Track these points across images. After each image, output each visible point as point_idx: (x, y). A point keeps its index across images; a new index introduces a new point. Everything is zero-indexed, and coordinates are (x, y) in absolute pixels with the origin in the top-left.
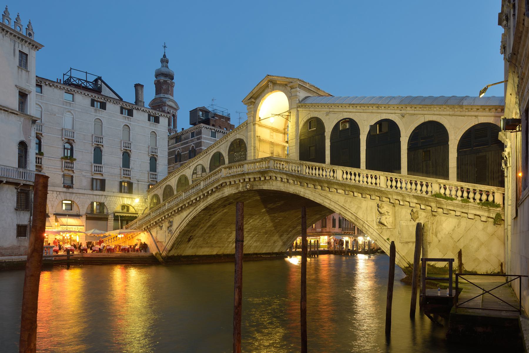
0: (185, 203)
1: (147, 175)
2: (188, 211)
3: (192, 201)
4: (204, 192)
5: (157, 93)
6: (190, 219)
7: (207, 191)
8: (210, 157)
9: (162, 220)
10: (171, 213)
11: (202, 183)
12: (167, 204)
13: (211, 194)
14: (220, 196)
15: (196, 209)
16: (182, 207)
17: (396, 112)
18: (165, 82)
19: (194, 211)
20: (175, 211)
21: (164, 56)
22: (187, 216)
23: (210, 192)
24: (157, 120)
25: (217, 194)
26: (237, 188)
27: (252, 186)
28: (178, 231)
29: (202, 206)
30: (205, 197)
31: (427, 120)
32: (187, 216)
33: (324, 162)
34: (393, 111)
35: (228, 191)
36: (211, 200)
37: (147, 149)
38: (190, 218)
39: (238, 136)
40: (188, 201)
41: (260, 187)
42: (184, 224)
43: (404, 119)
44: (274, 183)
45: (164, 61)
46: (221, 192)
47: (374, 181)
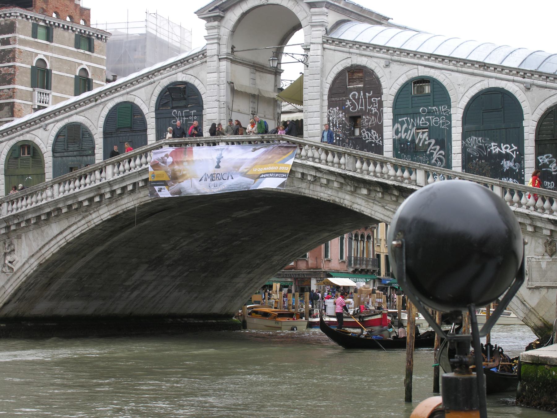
0: (60, 206)
2: (65, 224)
3: (81, 202)
4: (115, 188)
6: (70, 238)
10: (19, 224)
13: (133, 191)
15: (87, 219)
16: (49, 214)
17: (516, 78)
19: (83, 222)
20: (28, 221)
22: (61, 233)
23: (130, 188)
28: (34, 264)
29: (104, 213)
30: (114, 197)
32: (61, 233)
34: (511, 78)
36: (128, 203)
39: (181, 77)
40: (69, 202)
42: (54, 248)
43: (529, 93)
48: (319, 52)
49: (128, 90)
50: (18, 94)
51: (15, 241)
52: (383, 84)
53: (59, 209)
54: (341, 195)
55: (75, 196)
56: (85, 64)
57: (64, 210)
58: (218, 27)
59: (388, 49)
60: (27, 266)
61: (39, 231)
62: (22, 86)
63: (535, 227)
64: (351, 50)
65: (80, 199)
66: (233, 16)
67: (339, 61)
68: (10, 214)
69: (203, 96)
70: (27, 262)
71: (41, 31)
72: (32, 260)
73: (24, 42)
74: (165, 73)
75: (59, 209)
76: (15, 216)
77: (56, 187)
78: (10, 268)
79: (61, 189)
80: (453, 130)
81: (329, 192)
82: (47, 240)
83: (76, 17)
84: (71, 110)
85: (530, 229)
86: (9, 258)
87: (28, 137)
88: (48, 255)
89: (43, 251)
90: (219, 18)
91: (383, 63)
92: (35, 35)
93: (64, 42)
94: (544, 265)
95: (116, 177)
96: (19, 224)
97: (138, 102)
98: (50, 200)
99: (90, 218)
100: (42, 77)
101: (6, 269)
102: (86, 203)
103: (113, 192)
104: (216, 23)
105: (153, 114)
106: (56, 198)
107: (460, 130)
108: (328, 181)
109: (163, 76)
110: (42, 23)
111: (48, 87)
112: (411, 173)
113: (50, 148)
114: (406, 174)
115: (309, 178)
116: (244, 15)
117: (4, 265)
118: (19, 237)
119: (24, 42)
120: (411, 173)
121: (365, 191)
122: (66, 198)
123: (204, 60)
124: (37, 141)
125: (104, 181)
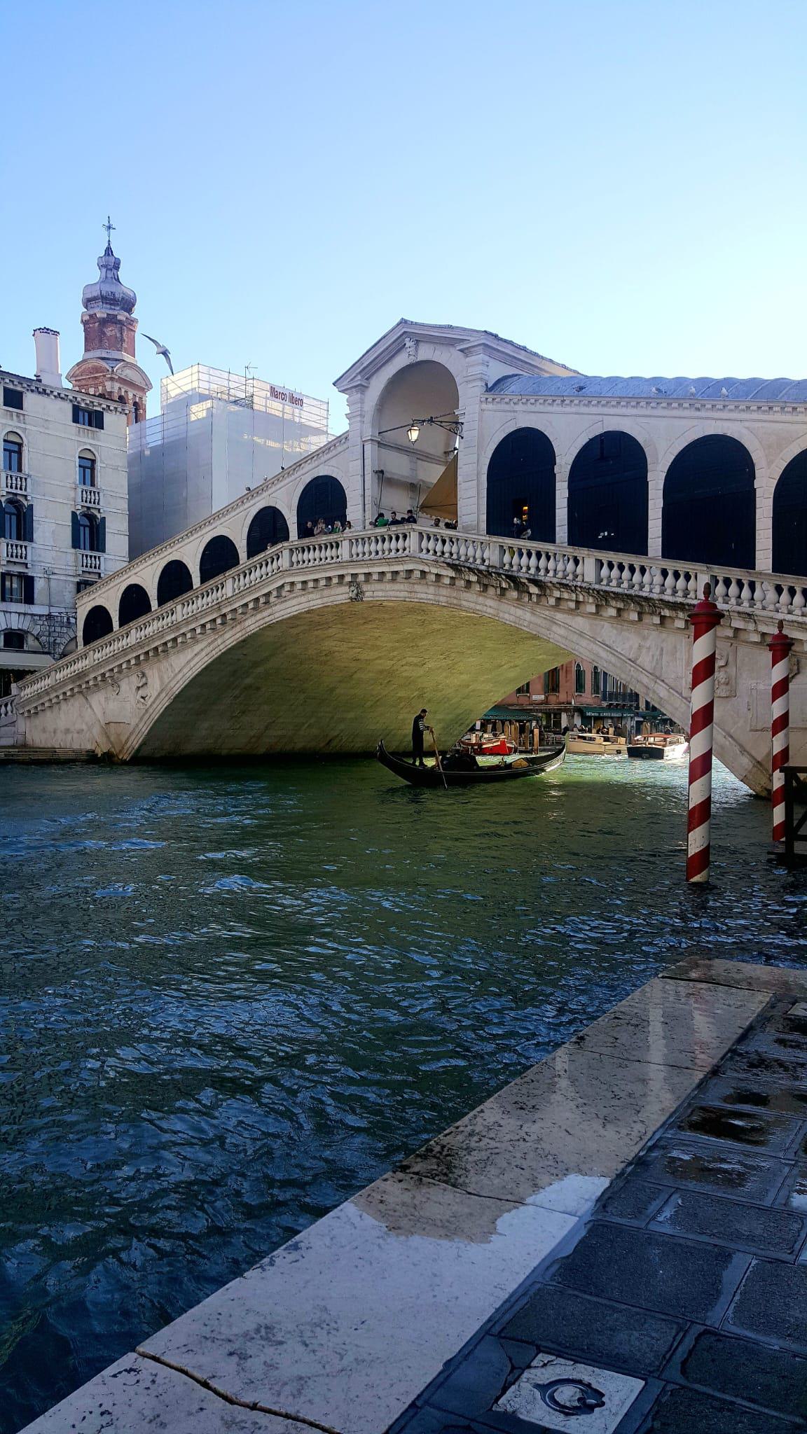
5: (87, 350)
9: (120, 672)
11: (229, 583)
12: (133, 631)
18: (111, 320)
20: (156, 649)
21: (109, 251)
24: (96, 420)
33: (552, 539)
36: (252, 624)
39: (323, 471)
45: (110, 264)
49: (270, 491)
58: (362, 401)
64: (517, 408)
90: (362, 388)
109: (305, 470)
123: (345, 446)
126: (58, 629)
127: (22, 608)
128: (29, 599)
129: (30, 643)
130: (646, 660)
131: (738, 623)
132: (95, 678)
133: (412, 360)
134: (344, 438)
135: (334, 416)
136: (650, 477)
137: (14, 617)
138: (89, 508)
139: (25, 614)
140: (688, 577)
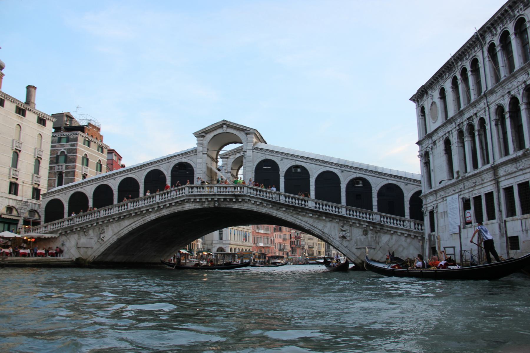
0: (131, 212)
1: (31, 177)
2: (131, 221)
3: (142, 211)
4: (160, 205)
6: (134, 227)
7: (165, 204)
8: (145, 173)
14: (178, 210)
15: (144, 219)
16: (125, 216)
19: (142, 220)
20: (114, 219)
22: (130, 225)
23: (168, 205)
25: (173, 208)
26: (202, 205)
27: (219, 204)
28: (115, 238)
31: (358, 176)
32: (130, 225)
35: (188, 207)
36: (165, 212)
37: (34, 151)
38: (134, 226)
39: (184, 160)
41: (230, 206)
42: (126, 231)
44: (246, 205)
46: (181, 207)
47: (337, 210)
48: (251, 153)
50: (77, 167)
51: (105, 228)
52: (280, 167)
53: (131, 214)
54: (271, 210)
55: (140, 208)
56: (100, 158)
57: (133, 215)
59: (282, 153)
60: (111, 239)
61: (118, 223)
62: (79, 164)
63: (360, 224)
65: (142, 210)
66: (210, 136)
67: (260, 157)
68: (104, 216)
69: (194, 169)
70: (111, 237)
71: (87, 143)
72: (114, 236)
73: (81, 146)
74: (176, 158)
75: (131, 214)
76: (107, 217)
77: (129, 204)
78: (102, 240)
79: (132, 205)
80: (311, 186)
81: (266, 209)
82: (122, 228)
83: (98, 139)
84: (128, 172)
85: (358, 225)
86: (102, 235)
87: (105, 183)
88: (122, 235)
89: (120, 233)
91: (280, 159)
92: (84, 144)
93: (94, 146)
94: (362, 240)
95: (161, 200)
96: (109, 220)
97: (162, 170)
98: (126, 210)
99: (145, 218)
100: (86, 161)
101: (100, 240)
102: (144, 212)
103: (159, 207)
104: (202, 139)
105: (170, 175)
106: (129, 208)
107: (314, 187)
108: (267, 204)
110: (87, 139)
111: (87, 165)
112: (305, 202)
113: (117, 188)
114: (303, 202)
115: (258, 203)
116: (215, 136)
117: (100, 238)
118: (107, 226)
119: (80, 145)
120: (305, 202)
121: (284, 209)
122: (135, 209)
124: (110, 185)
125: (154, 202)
126: (24, 207)
127: (13, 196)
128: (16, 193)
129: (15, 213)
130: (326, 231)
131: (354, 221)
132: (76, 229)
133: (225, 131)
134: (194, 151)
135: (192, 143)
136: (311, 179)
137: (11, 200)
138: (38, 157)
139: (14, 200)
140: (339, 208)
